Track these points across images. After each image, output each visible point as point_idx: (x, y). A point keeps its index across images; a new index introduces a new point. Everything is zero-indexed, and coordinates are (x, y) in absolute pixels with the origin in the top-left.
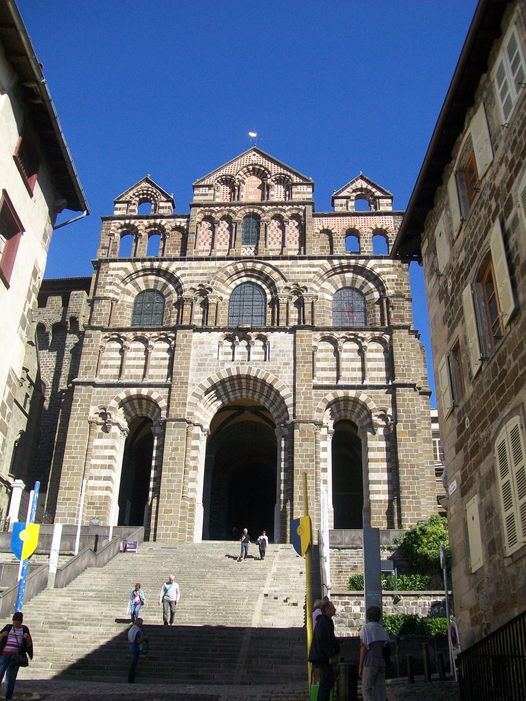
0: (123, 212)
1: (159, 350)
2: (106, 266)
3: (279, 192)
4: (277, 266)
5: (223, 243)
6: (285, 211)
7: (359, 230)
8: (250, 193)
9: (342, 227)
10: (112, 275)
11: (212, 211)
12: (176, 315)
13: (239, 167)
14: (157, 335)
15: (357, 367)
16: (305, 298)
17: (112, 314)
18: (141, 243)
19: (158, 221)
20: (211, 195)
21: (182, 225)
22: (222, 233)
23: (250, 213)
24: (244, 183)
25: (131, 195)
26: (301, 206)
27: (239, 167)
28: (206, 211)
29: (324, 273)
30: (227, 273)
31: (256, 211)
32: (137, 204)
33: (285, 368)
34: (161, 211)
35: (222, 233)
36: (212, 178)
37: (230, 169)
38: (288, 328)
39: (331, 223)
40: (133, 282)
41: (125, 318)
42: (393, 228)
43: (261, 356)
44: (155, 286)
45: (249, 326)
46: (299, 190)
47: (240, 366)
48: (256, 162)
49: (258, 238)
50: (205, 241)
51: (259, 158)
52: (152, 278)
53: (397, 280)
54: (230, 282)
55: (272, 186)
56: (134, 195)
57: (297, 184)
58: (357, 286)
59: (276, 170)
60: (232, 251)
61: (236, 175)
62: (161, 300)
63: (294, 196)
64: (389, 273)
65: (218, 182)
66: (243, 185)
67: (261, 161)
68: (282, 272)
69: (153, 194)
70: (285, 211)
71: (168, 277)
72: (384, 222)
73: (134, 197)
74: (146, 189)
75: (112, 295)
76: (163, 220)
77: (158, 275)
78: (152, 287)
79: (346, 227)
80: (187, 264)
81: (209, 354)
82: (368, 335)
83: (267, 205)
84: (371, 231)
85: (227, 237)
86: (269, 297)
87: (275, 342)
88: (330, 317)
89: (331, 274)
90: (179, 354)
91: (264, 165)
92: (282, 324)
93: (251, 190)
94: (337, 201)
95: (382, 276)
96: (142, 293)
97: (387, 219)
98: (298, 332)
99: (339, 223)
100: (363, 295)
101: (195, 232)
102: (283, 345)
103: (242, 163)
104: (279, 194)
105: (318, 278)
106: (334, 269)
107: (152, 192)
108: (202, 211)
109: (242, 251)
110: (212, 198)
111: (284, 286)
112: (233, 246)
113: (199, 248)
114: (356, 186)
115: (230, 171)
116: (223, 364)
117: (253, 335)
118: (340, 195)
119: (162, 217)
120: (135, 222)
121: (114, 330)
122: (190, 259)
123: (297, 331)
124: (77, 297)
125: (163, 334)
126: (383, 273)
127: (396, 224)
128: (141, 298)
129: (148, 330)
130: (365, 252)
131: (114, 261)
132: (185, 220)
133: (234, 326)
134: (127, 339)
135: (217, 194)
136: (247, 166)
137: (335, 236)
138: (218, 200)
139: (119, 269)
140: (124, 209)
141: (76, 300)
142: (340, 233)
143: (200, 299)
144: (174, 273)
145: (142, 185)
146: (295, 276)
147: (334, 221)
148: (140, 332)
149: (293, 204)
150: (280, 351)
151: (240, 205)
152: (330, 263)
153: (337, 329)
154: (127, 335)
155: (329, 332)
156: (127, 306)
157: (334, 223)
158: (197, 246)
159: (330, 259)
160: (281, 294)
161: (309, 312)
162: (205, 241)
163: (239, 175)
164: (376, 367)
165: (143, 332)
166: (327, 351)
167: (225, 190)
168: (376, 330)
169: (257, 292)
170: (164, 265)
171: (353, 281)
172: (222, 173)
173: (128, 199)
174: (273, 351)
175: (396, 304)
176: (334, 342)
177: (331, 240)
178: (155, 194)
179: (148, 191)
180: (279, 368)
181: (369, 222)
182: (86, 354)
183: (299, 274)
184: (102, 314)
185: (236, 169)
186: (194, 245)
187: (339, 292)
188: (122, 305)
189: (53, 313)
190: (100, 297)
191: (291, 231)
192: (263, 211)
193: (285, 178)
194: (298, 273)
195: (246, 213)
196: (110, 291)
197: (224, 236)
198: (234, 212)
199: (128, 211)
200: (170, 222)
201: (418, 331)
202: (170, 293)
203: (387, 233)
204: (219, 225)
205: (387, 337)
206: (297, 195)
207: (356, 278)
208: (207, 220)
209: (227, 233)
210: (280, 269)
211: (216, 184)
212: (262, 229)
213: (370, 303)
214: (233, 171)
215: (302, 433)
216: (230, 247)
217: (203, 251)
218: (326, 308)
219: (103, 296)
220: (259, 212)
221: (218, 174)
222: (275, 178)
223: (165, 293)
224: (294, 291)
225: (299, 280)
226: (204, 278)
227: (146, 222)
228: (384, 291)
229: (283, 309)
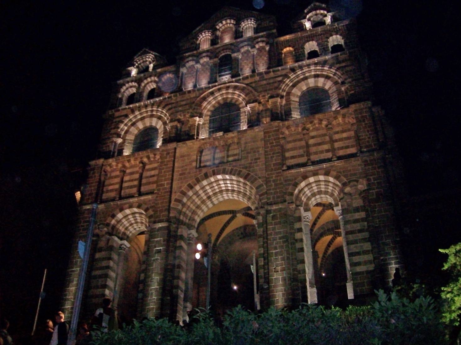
10: (116, 122)
15: (324, 149)
33: (256, 162)
47: (215, 169)
87: (246, 143)
90: (163, 169)
116: (200, 171)
150: (252, 149)
164: (344, 145)
180: (251, 163)
215: (274, 217)
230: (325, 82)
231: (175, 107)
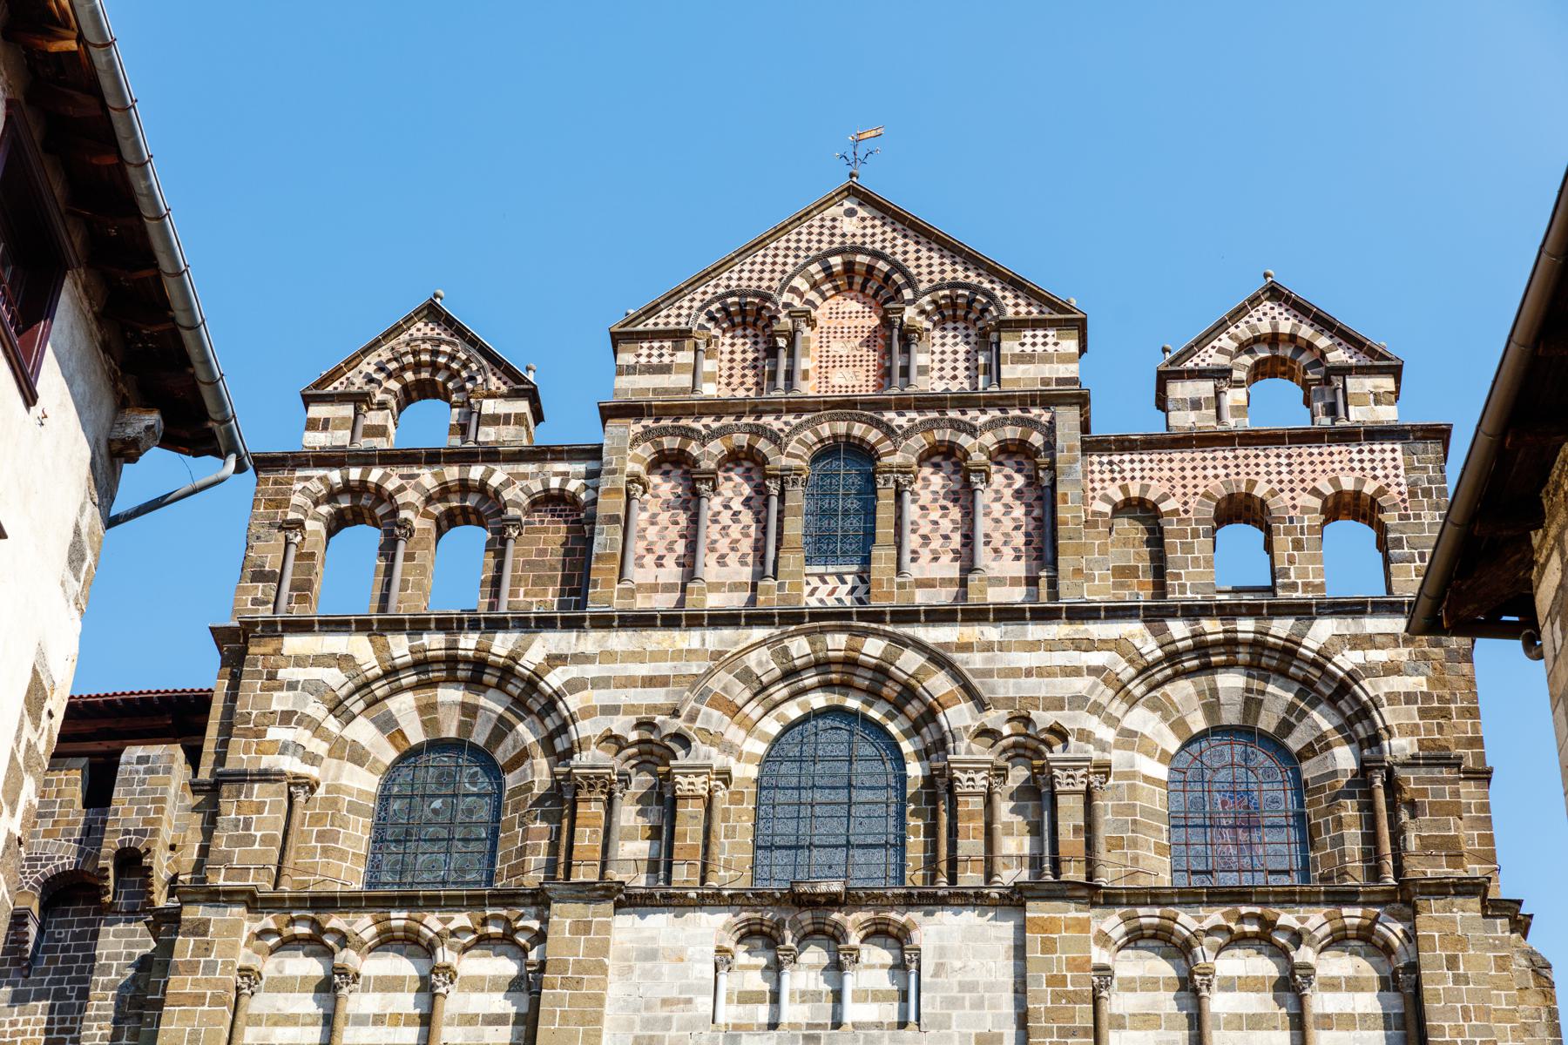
0: (341, 437)
1: (477, 984)
2: (269, 649)
3: (949, 357)
4: (946, 645)
5: (732, 559)
6: (972, 431)
7: (1270, 501)
8: (838, 362)
9: (1201, 490)
10: (292, 686)
11: (688, 434)
12: (544, 842)
13: (791, 260)
14: (469, 924)
16: (1057, 772)
17: (292, 839)
18: (409, 557)
19: (476, 472)
20: (682, 368)
21: (573, 485)
22: (726, 517)
23: (835, 436)
24: (812, 323)
25: (371, 369)
26: (1035, 412)
27: (791, 260)
28: (664, 432)
29: (1132, 671)
30: (746, 676)
31: (858, 430)
32: (393, 403)
34: (488, 434)
35: (726, 517)
36: (686, 304)
37: (757, 267)
38: (994, 894)
39: (1156, 474)
40: (375, 711)
41: (342, 855)
42: (1403, 489)
43: (885, 1005)
44: (465, 727)
45: (836, 887)
46: (1028, 349)
48: (859, 240)
49: (870, 536)
50: (660, 549)
51: (868, 223)
52: (450, 695)
53: (1427, 697)
54: (760, 710)
55: (920, 333)
56: (381, 369)
57: (1018, 325)
58: (1268, 722)
59: (936, 269)
60: (768, 590)
61: (781, 294)
62: (484, 783)
63: (1008, 371)
64: (1392, 669)
65: (711, 318)
66: (807, 331)
67: (879, 238)
68: (963, 668)
69: (455, 366)
70: (972, 431)
71: (516, 692)
72: (1367, 465)
73: (381, 376)
74: (428, 346)
75: (291, 764)
76: (497, 468)
77: (475, 683)
78: (450, 731)
79: (1216, 488)
80: (590, 641)
81: (677, 1002)
82: (1316, 919)
83: (902, 405)
84: (1317, 503)
85: (747, 536)
86: (915, 770)
87: (941, 951)
88: (1160, 850)
89: (1159, 677)
91: (888, 251)
92: (970, 877)
93: (837, 347)
94: (1179, 390)
95: (1365, 683)
96: (410, 755)
97: (1378, 456)
98: (1035, 910)
99: (1189, 473)
100: (1292, 760)
101: (622, 514)
102: (973, 963)
103: (803, 245)
104: (948, 365)
105: (1111, 692)
106: (1172, 657)
107: (452, 358)
108: (647, 435)
109: (807, 589)
110: (685, 380)
111: (974, 726)
112: (770, 570)
113: (636, 575)
114: (1252, 328)
115: (755, 276)
117: (853, 922)
118: (1189, 365)
119: (491, 455)
120: (386, 477)
121: (298, 902)
122: (603, 622)
123: (1029, 904)
124: (147, 772)
125: (495, 917)
126: (1370, 670)
127: (1414, 475)
128: (406, 774)
129: (433, 903)
130: (1294, 586)
131: (302, 627)
132: (581, 468)
133: (778, 886)
134: (353, 939)
135: (708, 366)
136: (822, 258)
137: (1170, 526)
138: (709, 390)
139: (319, 661)
140: (341, 423)
141: (143, 782)
142: (1191, 515)
143: (641, 782)
144: (538, 675)
145: (413, 330)
146: (1018, 687)
147: (1166, 465)
148: (404, 914)
149: (1002, 402)
150: (963, 987)
151: (798, 408)
152: (1154, 634)
153: (1189, 897)
154: (350, 924)
155: (1157, 911)
156: (354, 808)
157: (1167, 474)
158: (630, 568)
159: (1155, 616)
160: (962, 756)
161: (1076, 829)
162: (660, 549)
163: (794, 290)
165: (415, 915)
166: (1150, 984)
167: (738, 348)
168: (1347, 898)
169: (868, 750)
170: (502, 644)
171: (1248, 702)
172: (724, 282)
173: (359, 382)
174: (933, 988)
175: (1424, 793)
176: (1179, 949)
177: (1156, 540)
178: (465, 366)
179: (435, 353)
181: (1308, 468)
182: (182, 999)
183: (1034, 680)
184: (250, 840)
185: (778, 268)
186: (617, 567)
187: (1195, 748)
188: (332, 803)
189: (48, 833)
190: (245, 773)
191: (998, 509)
192: (889, 431)
193: (971, 302)
194: (1029, 673)
195: (821, 441)
196: (284, 749)
197: (735, 531)
198: (774, 438)
199: (359, 430)
200: (525, 476)
201: (1519, 903)
202: (523, 756)
203: (1382, 510)
204: (714, 489)
205: (1394, 931)
206: (1021, 367)
207: (1263, 693)
208: (666, 467)
209: (747, 517)
210: (958, 657)
211: (701, 327)
212: (885, 502)
213: (1320, 790)
214: (767, 275)
216: (760, 575)
217: (654, 588)
218: (1144, 811)
219: (253, 768)
220: (873, 436)
221: (710, 290)
222: (934, 302)
223: (502, 755)
224: (1015, 746)
225: (1034, 702)
226: (658, 696)
227: (427, 478)
228: (1374, 740)
229: (971, 816)
230: (1293, 720)
231: (600, 683)
